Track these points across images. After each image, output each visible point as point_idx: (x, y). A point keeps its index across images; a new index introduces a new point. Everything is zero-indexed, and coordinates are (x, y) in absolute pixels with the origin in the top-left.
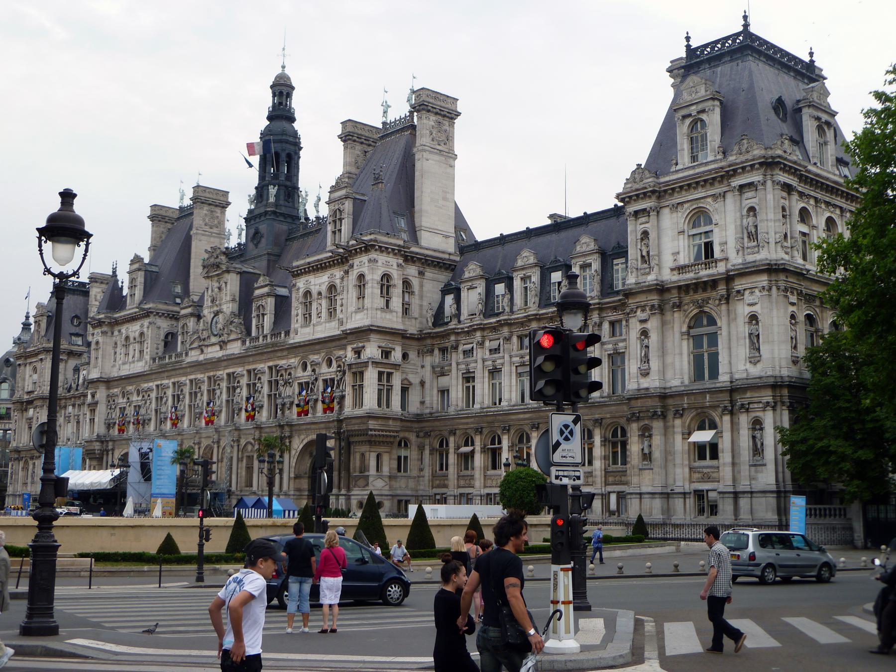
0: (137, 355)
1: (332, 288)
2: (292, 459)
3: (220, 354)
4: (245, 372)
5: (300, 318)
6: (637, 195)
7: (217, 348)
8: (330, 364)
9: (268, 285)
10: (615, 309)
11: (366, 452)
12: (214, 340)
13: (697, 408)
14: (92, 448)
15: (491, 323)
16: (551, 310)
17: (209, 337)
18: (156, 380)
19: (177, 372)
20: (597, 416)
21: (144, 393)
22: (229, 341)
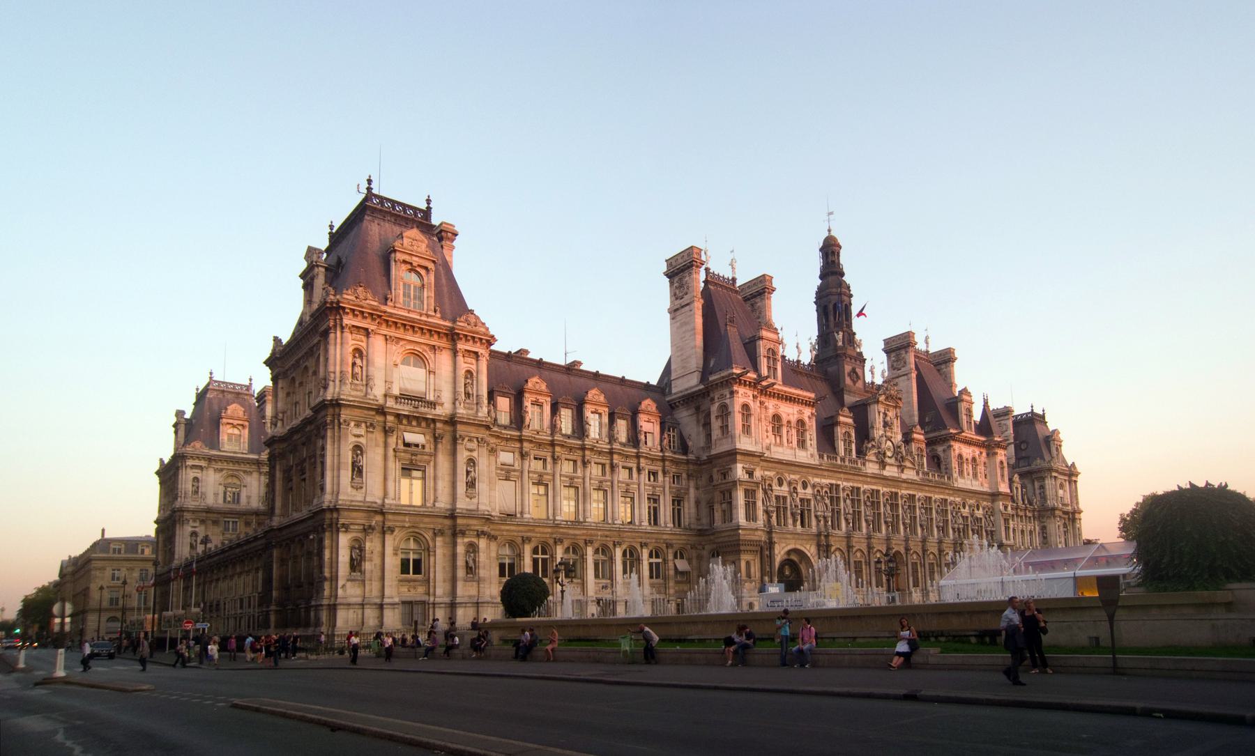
0: (795, 443)
1: (974, 459)
3: (904, 476)
7: (895, 469)
18: (829, 477)
19: (856, 478)
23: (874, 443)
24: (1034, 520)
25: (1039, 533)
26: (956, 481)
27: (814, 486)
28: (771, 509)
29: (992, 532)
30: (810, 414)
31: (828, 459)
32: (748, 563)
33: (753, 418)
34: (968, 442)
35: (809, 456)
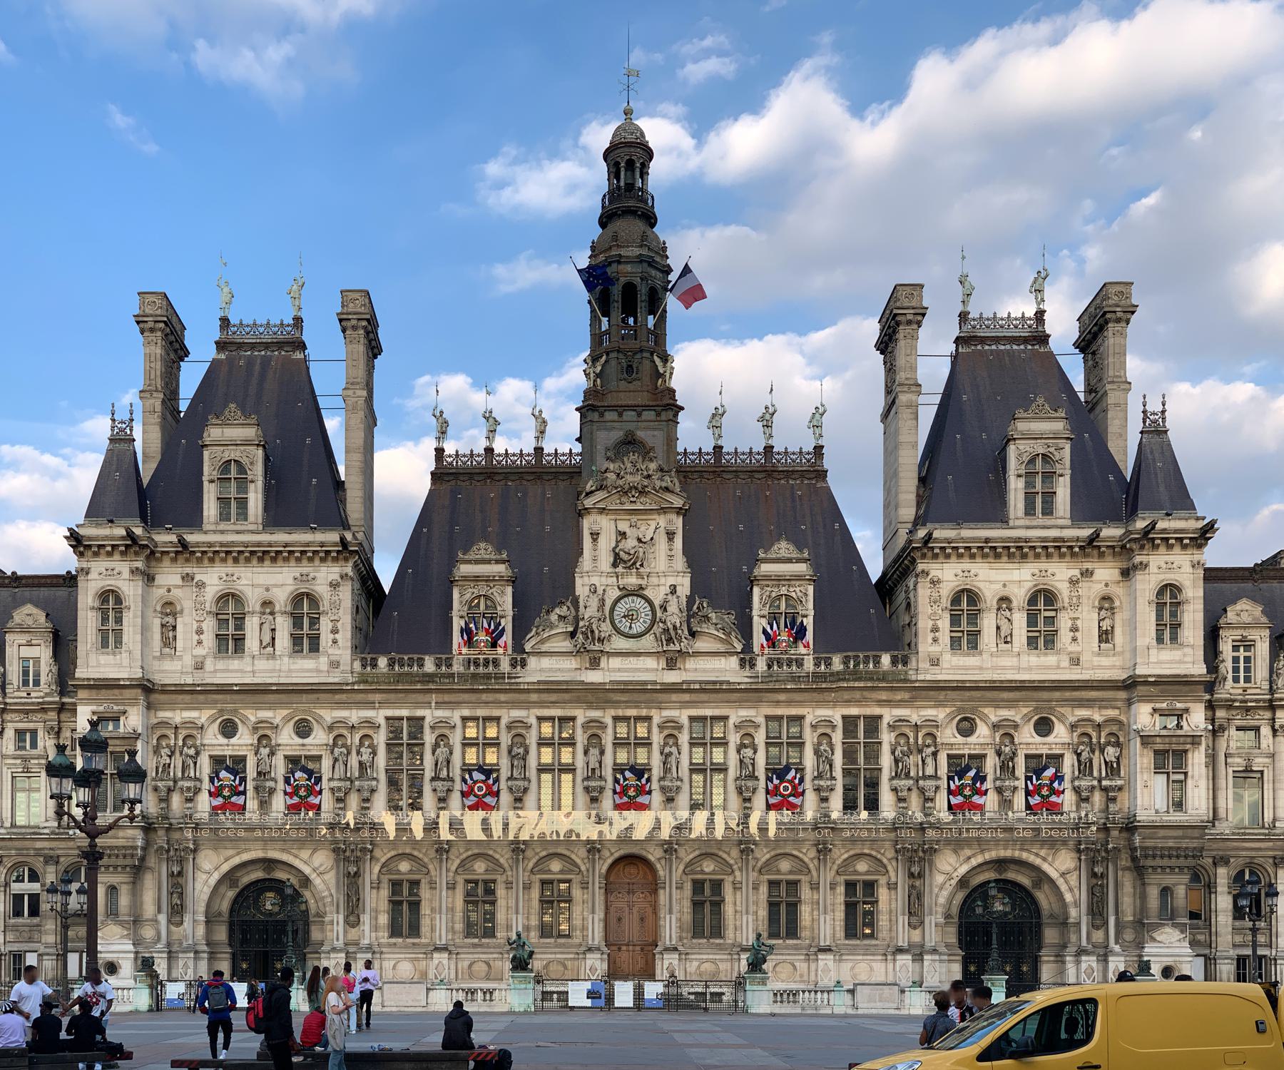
0: (283, 641)
1: (1043, 598)
2: (936, 890)
3: (672, 677)
4: (761, 720)
5: (945, 636)
7: (651, 663)
8: (1044, 727)
12: (620, 643)
14: (121, 842)
18: (383, 704)
19: (484, 697)
21: (345, 732)
26: (935, 662)
27: (331, 728)
28: (187, 784)
29: (1106, 790)
30: (337, 577)
31: (391, 664)
32: (112, 889)
33: (128, 618)
34: (1019, 551)
35: (324, 667)
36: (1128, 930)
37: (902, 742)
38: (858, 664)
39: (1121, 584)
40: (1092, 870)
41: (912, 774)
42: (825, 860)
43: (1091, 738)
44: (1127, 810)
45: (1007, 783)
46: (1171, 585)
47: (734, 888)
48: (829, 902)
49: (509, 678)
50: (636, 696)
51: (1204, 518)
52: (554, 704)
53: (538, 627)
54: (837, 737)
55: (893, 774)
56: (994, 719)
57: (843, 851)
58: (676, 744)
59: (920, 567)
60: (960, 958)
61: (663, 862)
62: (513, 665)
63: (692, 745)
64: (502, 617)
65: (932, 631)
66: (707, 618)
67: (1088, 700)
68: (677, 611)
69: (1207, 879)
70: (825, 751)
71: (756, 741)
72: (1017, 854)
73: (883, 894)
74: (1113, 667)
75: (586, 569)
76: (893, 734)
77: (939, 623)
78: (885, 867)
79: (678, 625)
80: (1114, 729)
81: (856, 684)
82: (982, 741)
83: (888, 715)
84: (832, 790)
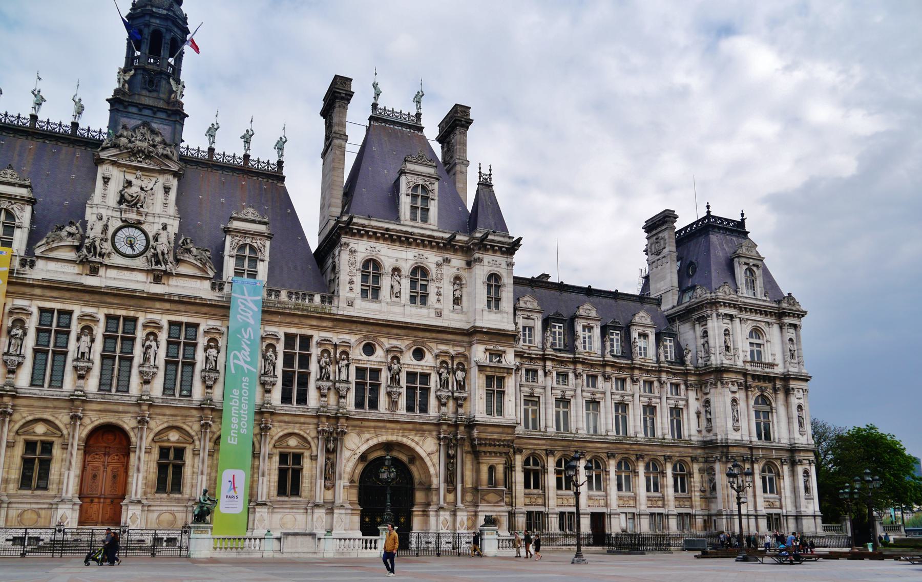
1: (420, 271)
2: (344, 462)
5: (357, 287)
6: (730, 304)
7: (141, 277)
8: (419, 354)
9: (268, 223)
10: (674, 374)
11: (497, 464)
12: (117, 260)
13: (766, 458)
15: (564, 357)
16: (622, 361)
17: (109, 254)
20: (668, 454)
22: (179, 275)
23: (73, 229)
24: (687, 389)
25: (698, 414)
26: (350, 304)
29: (456, 399)
34: (405, 240)
36: (469, 494)
37: (326, 355)
38: (299, 298)
39: (466, 270)
40: (448, 452)
41: (331, 378)
42: (266, 435)
43: (447, 364)
44: (469, 414)
45: (395, 390)
46: (495, 274)
47: (194, 454)
48: (266, 467)
49: (17, 273)
50: (126, 301)
51: (513, 238)
52: (55, 298)
53: (48, 238)
54: (280, 347)
55: (318, 377)
56: (387, 346)
57: (279, 430)
58: (156, 340)
59: (344, 240)
60: (359, 512)
61: (136, 431)
62: (23, 263)
63: (169, 343)
64: (18, 227)
65: (349, 283)
66: (189, 251)
67: (447, 340)
68: (166, 242)
69: (510, 462)
70: (271, 356)
71: (220, 344)
72: (400, 439)
73: (306, 463)
74: (461, 321)
75: (96, 202)
76: (319, 349)
77: (354, 279)
78: (309, 443)
79: (166, 252)
80: (462, 360)
81: (296, 312)
82: (379, 360)
83: (317, 336)
84: (274, 385)
